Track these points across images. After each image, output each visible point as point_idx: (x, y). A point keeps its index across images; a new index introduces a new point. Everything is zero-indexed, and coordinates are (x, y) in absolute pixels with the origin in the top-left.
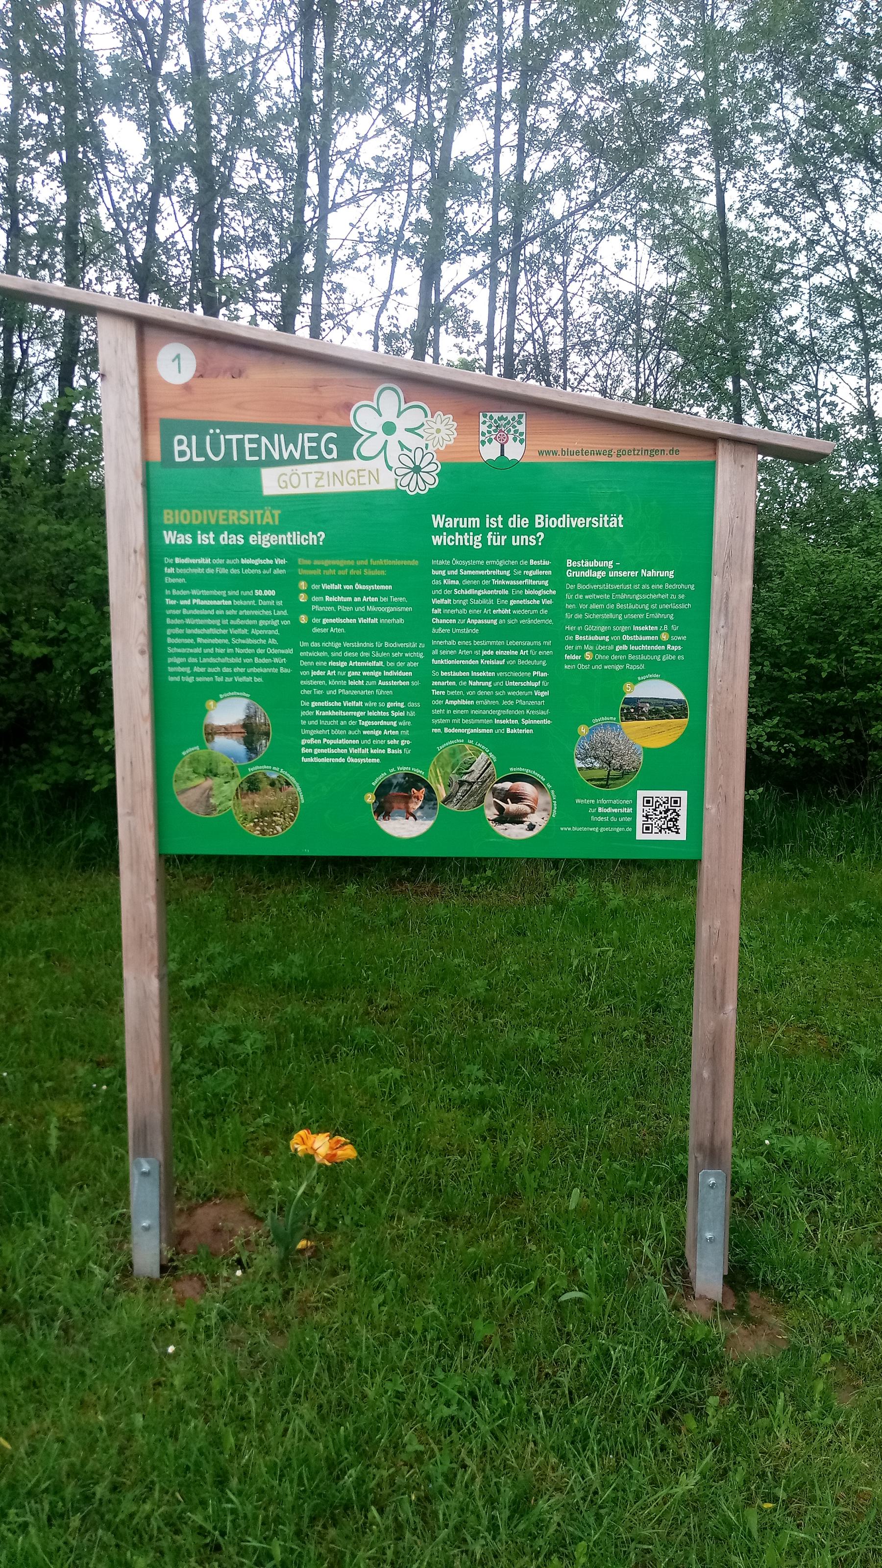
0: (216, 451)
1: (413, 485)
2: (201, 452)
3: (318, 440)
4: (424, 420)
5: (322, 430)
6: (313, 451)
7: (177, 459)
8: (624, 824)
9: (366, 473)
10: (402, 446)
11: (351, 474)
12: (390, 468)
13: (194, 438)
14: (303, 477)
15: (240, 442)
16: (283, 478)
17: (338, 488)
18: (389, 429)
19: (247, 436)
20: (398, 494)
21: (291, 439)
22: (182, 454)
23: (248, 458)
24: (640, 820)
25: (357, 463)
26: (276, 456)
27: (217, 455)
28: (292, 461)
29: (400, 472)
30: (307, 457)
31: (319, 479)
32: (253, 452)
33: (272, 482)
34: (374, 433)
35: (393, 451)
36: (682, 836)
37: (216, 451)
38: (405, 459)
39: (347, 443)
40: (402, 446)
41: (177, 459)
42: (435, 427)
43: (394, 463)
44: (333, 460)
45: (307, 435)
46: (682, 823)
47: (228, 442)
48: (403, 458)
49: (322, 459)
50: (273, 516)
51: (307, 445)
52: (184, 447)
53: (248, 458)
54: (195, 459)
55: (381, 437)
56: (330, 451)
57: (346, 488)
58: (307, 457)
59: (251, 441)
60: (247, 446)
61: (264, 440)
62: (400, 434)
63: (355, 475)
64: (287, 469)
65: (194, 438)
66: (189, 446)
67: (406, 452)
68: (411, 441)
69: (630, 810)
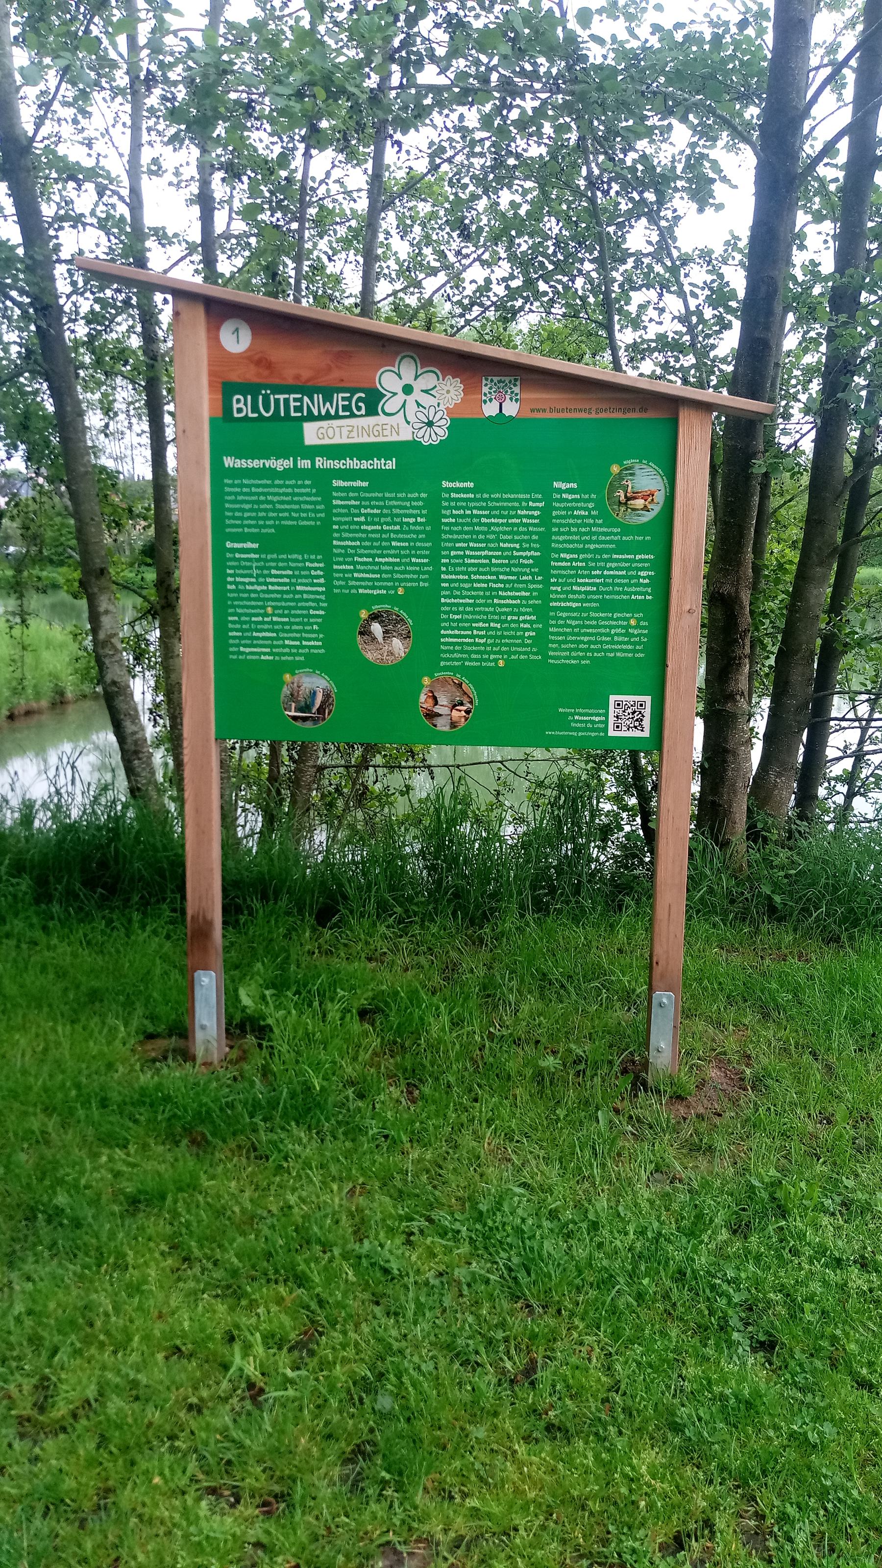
1: (426, 438)
2: (255, 409)
3: (349, 399)
6: (345, 408)
7: (236, 415)
8: (598, 730)
15: (287, 401)
18: (408, 390)
19: (292, 396)
21: (328, 398)
22: (240, 410)
23: (293, 414)
24: (612, 719)
25: (381, 419)
26: (316, 413)
27: (267, 411)
28: (328, 417)
29: (417, 426)
32: (297, 409)
33: (312, 433)
34: (395, 394)
35: (411, 407)
36: (646, 734)
38: (420, 415)
39: (373, 402)
41: (236, 415)
46: (646, 722)
47: (277, 401)
49: (352, 415)
51: (341, 403)
52: (241, 405)
53: (293, 414)
54: (250, 415)
55: (401, 397)
57: (372, 439)
59: (295, 400)
60: (292, 404)
61: (306, 399)
62: (417, 395)
64: (324, 424)
66: (246, 404)
69: (602, 726)
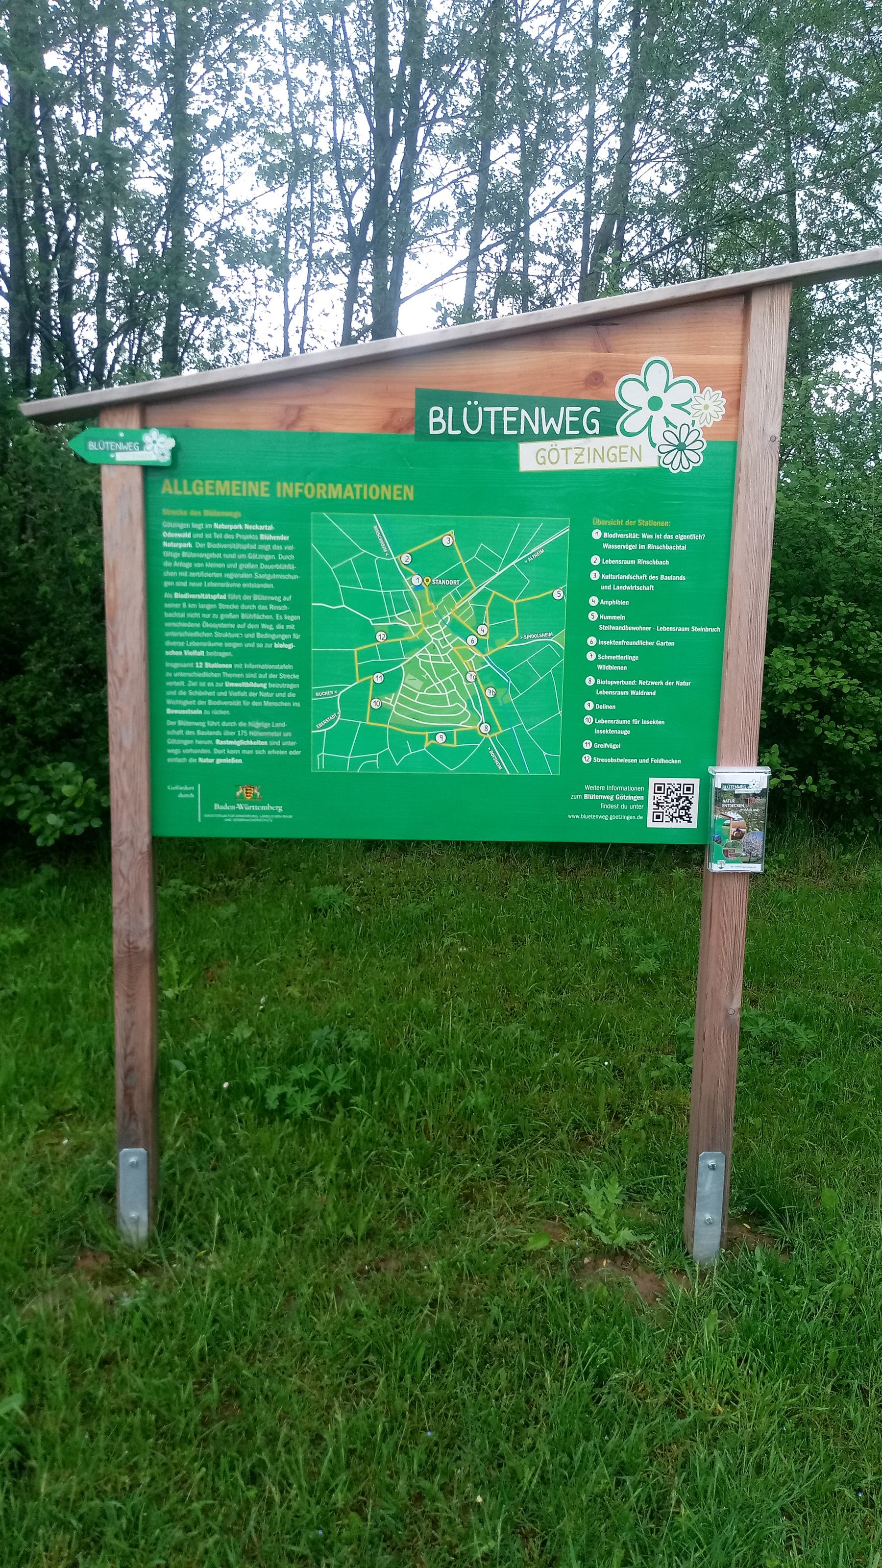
0: (473, 424)
1: (685, 463)
2: (458, 424)
3: (580, 414)
4: (692, 395)
5: (585, 405)
6: (574, 425)
7: (432, 432)
9: (628, 450)
10: (668, 422)
11: (613, 451)
12: (654, 445)
13: (451, 409)
14: (562, 453)
15: (499, 415)
16: (541, 453)
17: (598, 465)
18: (655, 403)
19: (506, 409)
20: (659, 473)
21: (552, 413)
22: (437, 426)
23: (506, 432)
25: (619, 439)
26: (536, 430)
27: (473, 428)
28: (552, 436)
29: (664, 449)
30: (568, 432)
31: (579, 455)
32: (511, 426)
33: (531, 458)
34: (639, 409)
35: (658, 426)
37: (473, 424)
38: (669, 436)
39: (609, 420)
40: (668, 422)
41: (432, 432)
42: (704, 403)
43: (658, 439)
44: (595, 435)
45: (569, 409)
47: (487, 415)
48: (667, 435)
49: (583, 435)
50: (354, 490)
51: (569, 419)
52: (440, 419)
53: (506, 432)
54: (451, 432)
55: (646, 412)
56: (591, 426)
57: (607, 465)
58: (568, 432)
59: (510, 414)
60: (506, 419)
61: (524, 413)
62: (666, 410)
63: (617, 451)
64: (546, 445)
65: (451, 409)
66: (445, 418)
67: (671, 428)
68: (678, 417)
